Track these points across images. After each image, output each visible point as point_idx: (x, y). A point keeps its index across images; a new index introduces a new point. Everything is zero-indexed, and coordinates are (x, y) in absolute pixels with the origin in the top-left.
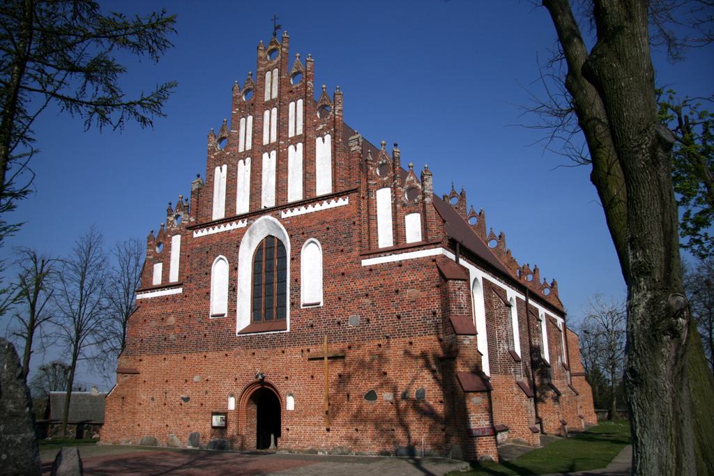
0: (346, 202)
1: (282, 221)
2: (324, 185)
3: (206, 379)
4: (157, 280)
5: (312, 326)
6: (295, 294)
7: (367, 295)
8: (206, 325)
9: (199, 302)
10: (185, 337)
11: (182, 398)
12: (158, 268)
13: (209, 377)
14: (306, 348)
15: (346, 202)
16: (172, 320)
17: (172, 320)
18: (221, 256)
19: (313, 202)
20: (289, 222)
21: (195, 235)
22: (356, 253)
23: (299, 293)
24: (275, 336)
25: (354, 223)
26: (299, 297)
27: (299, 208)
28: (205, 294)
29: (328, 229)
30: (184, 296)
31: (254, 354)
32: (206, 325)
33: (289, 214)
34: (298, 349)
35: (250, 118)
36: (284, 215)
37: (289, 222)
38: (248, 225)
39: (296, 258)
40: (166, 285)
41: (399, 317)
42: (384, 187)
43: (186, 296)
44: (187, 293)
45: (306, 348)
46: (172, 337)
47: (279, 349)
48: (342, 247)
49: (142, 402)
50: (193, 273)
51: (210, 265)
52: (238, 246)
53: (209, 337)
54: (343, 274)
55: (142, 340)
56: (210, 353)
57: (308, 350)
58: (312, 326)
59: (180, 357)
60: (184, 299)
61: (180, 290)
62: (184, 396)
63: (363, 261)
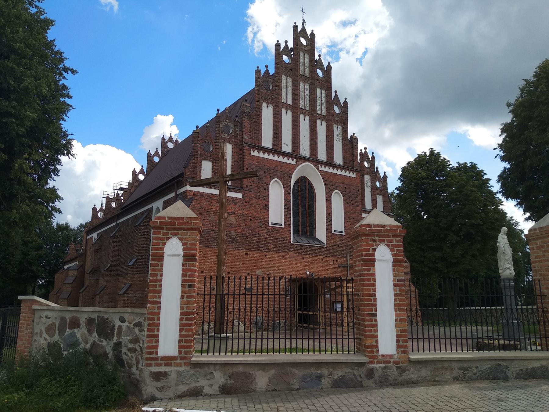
0: (354, 176)
1: (321, 172)
2: (338, 159)
3: (267, 273)
5: (338, 246)
6: (329, 223)
8: (266, 230)
9: (259, 210)
13: (271, 272)
14: (335, 259)
15: (354, 176)
18: (276, 179)
19: (338, 167)
20: (324, 174)
21: (252, 153)
22: (359, 208)
24: (317, 248)
25: (358, 190)
26: (331, 225)
27: (329, 167)
28: (265, 206)
29: (346, 188)
31: (303, 258)
32: (266, 230)
33: (322, 168)
34: (330, 259)
35: (290, 80)
36: (320, 169)
37: (324, 174)
38: (297, 165)
39: (328, 200)
42: (367, 174)
43: (246, 202)
44: (247, 199)
45: (335, 259)
47: (320, 258)
48: (353, 202)
50: (254, 185)
51: (268, 184)
52: (290, 177)
54: (354, 218)
56: (271, 253)
57: (337, 261)
58: (338, 246)
59: (242, 253)
60: (245, 204)
61: (239, 196)
63: (363, 214)
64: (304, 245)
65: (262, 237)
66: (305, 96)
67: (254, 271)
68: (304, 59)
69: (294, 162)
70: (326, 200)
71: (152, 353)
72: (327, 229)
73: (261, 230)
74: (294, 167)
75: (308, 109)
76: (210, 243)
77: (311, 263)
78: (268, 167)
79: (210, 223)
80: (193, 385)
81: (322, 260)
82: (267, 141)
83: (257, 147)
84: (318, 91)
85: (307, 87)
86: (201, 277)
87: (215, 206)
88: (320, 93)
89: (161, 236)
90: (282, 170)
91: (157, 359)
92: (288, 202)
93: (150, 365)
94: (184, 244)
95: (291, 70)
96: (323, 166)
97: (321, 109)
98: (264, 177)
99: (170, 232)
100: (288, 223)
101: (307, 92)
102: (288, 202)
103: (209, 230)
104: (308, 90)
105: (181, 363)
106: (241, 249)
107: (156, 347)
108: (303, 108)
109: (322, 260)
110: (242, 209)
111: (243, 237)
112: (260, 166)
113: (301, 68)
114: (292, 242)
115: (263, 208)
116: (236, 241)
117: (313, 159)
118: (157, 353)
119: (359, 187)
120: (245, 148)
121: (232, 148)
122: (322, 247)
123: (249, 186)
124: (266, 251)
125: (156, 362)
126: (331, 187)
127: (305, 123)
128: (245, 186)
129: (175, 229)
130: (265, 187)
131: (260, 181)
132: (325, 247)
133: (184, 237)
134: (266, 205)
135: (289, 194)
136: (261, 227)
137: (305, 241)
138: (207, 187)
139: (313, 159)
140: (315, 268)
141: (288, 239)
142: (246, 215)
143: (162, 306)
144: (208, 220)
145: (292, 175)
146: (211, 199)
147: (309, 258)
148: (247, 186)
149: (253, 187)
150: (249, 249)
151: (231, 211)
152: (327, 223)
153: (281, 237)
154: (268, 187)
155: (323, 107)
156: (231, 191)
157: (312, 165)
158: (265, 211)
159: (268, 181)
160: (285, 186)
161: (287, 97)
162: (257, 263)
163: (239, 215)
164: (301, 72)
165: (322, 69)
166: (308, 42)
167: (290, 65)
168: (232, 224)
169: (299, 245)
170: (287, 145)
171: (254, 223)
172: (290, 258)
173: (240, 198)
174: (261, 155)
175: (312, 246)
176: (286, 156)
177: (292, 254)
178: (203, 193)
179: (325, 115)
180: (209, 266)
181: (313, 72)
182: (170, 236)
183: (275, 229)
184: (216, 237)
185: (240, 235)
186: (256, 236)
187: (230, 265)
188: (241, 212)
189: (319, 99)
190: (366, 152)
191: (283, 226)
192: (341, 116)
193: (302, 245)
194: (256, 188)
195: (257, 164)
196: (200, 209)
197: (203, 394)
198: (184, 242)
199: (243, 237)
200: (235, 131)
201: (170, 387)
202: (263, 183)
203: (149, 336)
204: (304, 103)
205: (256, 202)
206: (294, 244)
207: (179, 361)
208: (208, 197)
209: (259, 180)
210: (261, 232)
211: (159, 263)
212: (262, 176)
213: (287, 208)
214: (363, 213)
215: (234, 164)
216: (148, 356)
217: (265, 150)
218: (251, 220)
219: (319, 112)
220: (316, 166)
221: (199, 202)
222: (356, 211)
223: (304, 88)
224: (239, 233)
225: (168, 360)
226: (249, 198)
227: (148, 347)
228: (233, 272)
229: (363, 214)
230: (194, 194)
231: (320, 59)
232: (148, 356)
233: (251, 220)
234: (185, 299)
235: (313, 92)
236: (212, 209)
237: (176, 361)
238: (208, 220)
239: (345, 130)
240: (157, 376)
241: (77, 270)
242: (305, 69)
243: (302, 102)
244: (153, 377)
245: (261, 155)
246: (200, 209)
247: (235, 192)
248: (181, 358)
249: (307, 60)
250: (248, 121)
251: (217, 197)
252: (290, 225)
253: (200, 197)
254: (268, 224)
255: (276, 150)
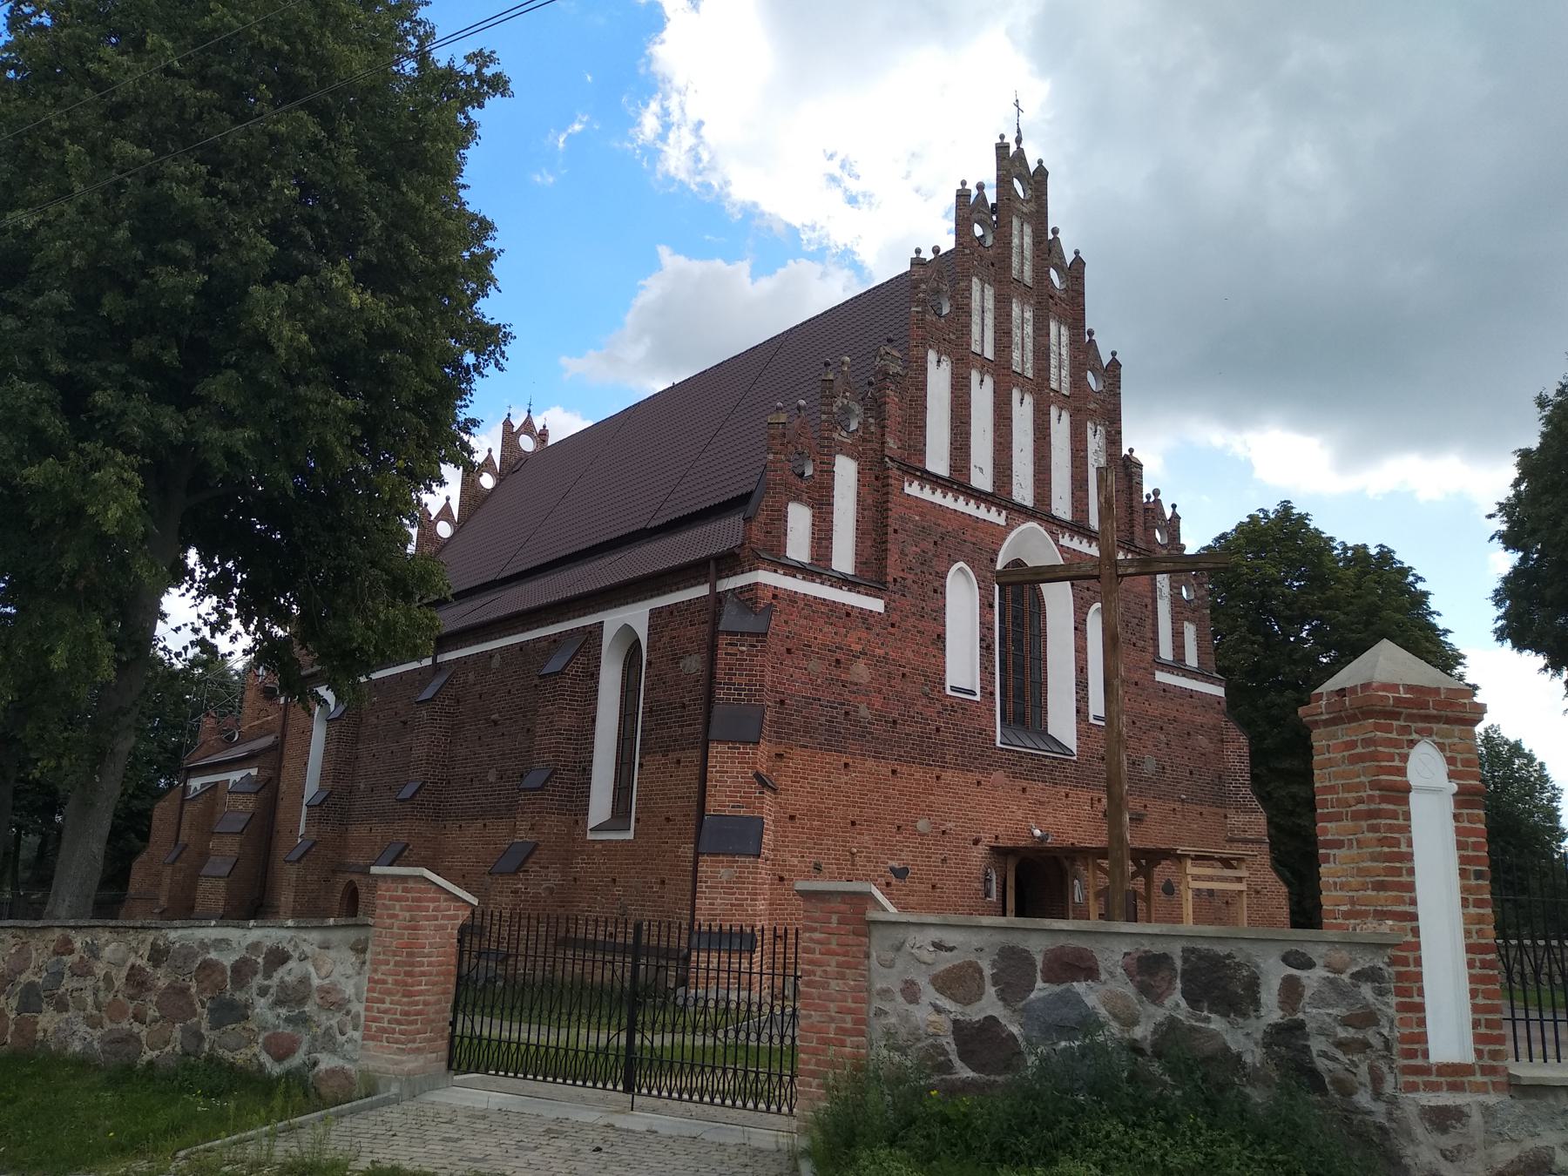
1: (1062, 548)
3: (943, 828)
4: (798, 547)
7: (1161, 728)
10: (895, 722)
11: (892, 870)
12: (799, 518)
13: (950, 825)
16: (861, 671)
17: (861, 671)
21: (908, 490)
22: (1149, 657)
23: (1087, 694)
28: (935, 637)
30: (887, 622)
31: (1024, 790)
32: (938, 706)
33: (1065, 541)
35: (989, 292)
36: (1062, 542)
38: (1009, 527)
40: (818, 569)
41: (1191, 773)
43: (893, 625)
44: (895, 617)
46: (864, 711)
47: (1063, 790)
48: (1134, 640)
49: (786, 875)
50: (911, 577)
53: (946, 735)
54: (1136, 684)
55: (782, 702)
60: (892, 630)
61: (876, 605)
62: (895, 864)
63: (1157, 673)
64: (1025, 753)
65: (929, 724)
66: (1023, 339)
67: (912, 822)
68: (1022, 238)
69: (1001, 521)
70: (1076, 629)
71: (1411, 1054)
72: (1078, 712)
73: (927, 707)
74: (1000, 534)
75: (1030, 375)
76: (811, 737)
77: (1042, 803)
78: (944, 530)
79: (810, 680)
80: (1530, 1144)
81: (1067, 796)
82: (938, 461)
83: (919, 474)
84: (1053, 327)
85: (1028, 315)
86: (790, 832)
87: (821, 630)
88: (1058, 334)
89: (1394, 735)
90: (974, 540)
91: (1425, 1071)
92: (988, 629)
93: (1413, 1087)
94: (1450, 761)
95: (993, 265)
96: (1067, 535)
97: (1060, 379)
98: (934, 555)
99: (1413, 726)
100: (990, 689)
101: (1029, 329)
102: (988, 629)
103: (809, 698)
104: (1031, 323)
105: (1485, 1083)
106: (883, 758)
107: (1422, 1038)
108: (1019, 370)
109: (1067, 796)
110: (882, 644)
111: (886, 721)
112: (926, 524)
113: (1015, 260)
114: (998, 744)
115: (933, 643)
116: (870, 733)
117: (1041, 512)
118: (1426, 1054)
119: (1146, 597)
120: (890, 473)
121: (859, 473)
122: (1067, 760)
123: (899, 580)
124: (939, 766)
125: (1426, 1078)
126: (1086, 594)
127: (1023, 413)
128: (890, 579)
129: (1427, 718)
130: (936, 584)
131: (925, 568)
132: (1074, 761)
133: (1447, 741)
134: (939, 636)
135: (991, 606)
136: (926, 695)
137: (1026, 745)
138: (804, 579)
139: (1041, 512)
140: (1050, 820)
141: (989, 735)
142: (894, 660)
143: (1422, 923)
144: (806, 669)
145: (997, 555)
146: (813, 611)
147: (1037, 788)
148: (895, 580)
149: (909, 582)
150: (899, 759)
151: (859, 648)
152: (1077, 693)
153: (974, 728)
154: (944, 586)
155: (1064, 373)
156: (859, 592)
157: (1042, 529)
158: (935, 652)
159: (943, 569)
160: (982, 585)
161: (983, 341)
162: (919, 797)
163: (877, 661)
164: (1015, 274)
165: (1060, 269)
166: (1030, 192)
167: (991, 252)
168: (861, 684)
169: (1014, 751)
170: (981, 469)
171: (911, 685)
172: (995, 788)
173: (880, 614)
174: (926, 494)
175: (1044, 756)
176: (985, 501)
177: (998, 776)
178: (796, 593)
179: (1067, 393)
180: (808, 801)
181: (1041, 276)
182: (1415, 736)
183: (960, 704)
184: (824, 718)
185: (880, 716)
186: (916, 722)
187: (857, 802)
188: (882, 652)
189: (1055, 348)
190: (1158, 502)
191: (977, 698)
192: (1103, 401)
193: (1021, 752)
194: (915, 586)
195: (917, 518)
196: (788, 637)
197: (1554, 1169)
198: (1448, 754)
199: (886, 721)
200: (864, 425)
201: (1474, 1150)
202: (931, 574)
203: (1402, 1007)
204: (1022, 359)
205: (915, 627)
206: (1002, 749)
207: (1479, 1078)
208: (806, 605)
209: (922, 564)
210: (928, 713)
211: (1400, 809)
212: (930, 554)
213: (986, 648)
214: (1157, 669)
215: (863, 518)
216: (1406, 1062)
217: (935, 481)
218: (904, 675)
219: (1054, 385)
220: (1051, 533)
221: (784, 617)
222: (1142, 665)
223: (1022, 315)
224: (876, 710)
225: (1454, 1074)
226: (899, 613)
227: (1405, 1039)
228: (865, 821)
229: (1157, 673)
230: (775, 597)
231: (1056, 239)
232: (1406, 1062)
233: (904, 675)
234: (1472, 910)
235: (1041, 331)
236: (815, 638)
237: (1471, 1078)
238: (806, 669)
239: (1114, 439)
240: (1442, 1119)
241: (256, 793)
242: (1023, 265)
243: (1016, 355)
244: (1430, 1121)
245: (926, 494)
246: (788, 637)
247: (867, 594)
248: (1486, 1071)
249: (1028, 240)
250: (897, 400)
251: (828, 605)
252: (992, 694)
253: (788, 605)
254: (944, 689)
255: (957, 483)
